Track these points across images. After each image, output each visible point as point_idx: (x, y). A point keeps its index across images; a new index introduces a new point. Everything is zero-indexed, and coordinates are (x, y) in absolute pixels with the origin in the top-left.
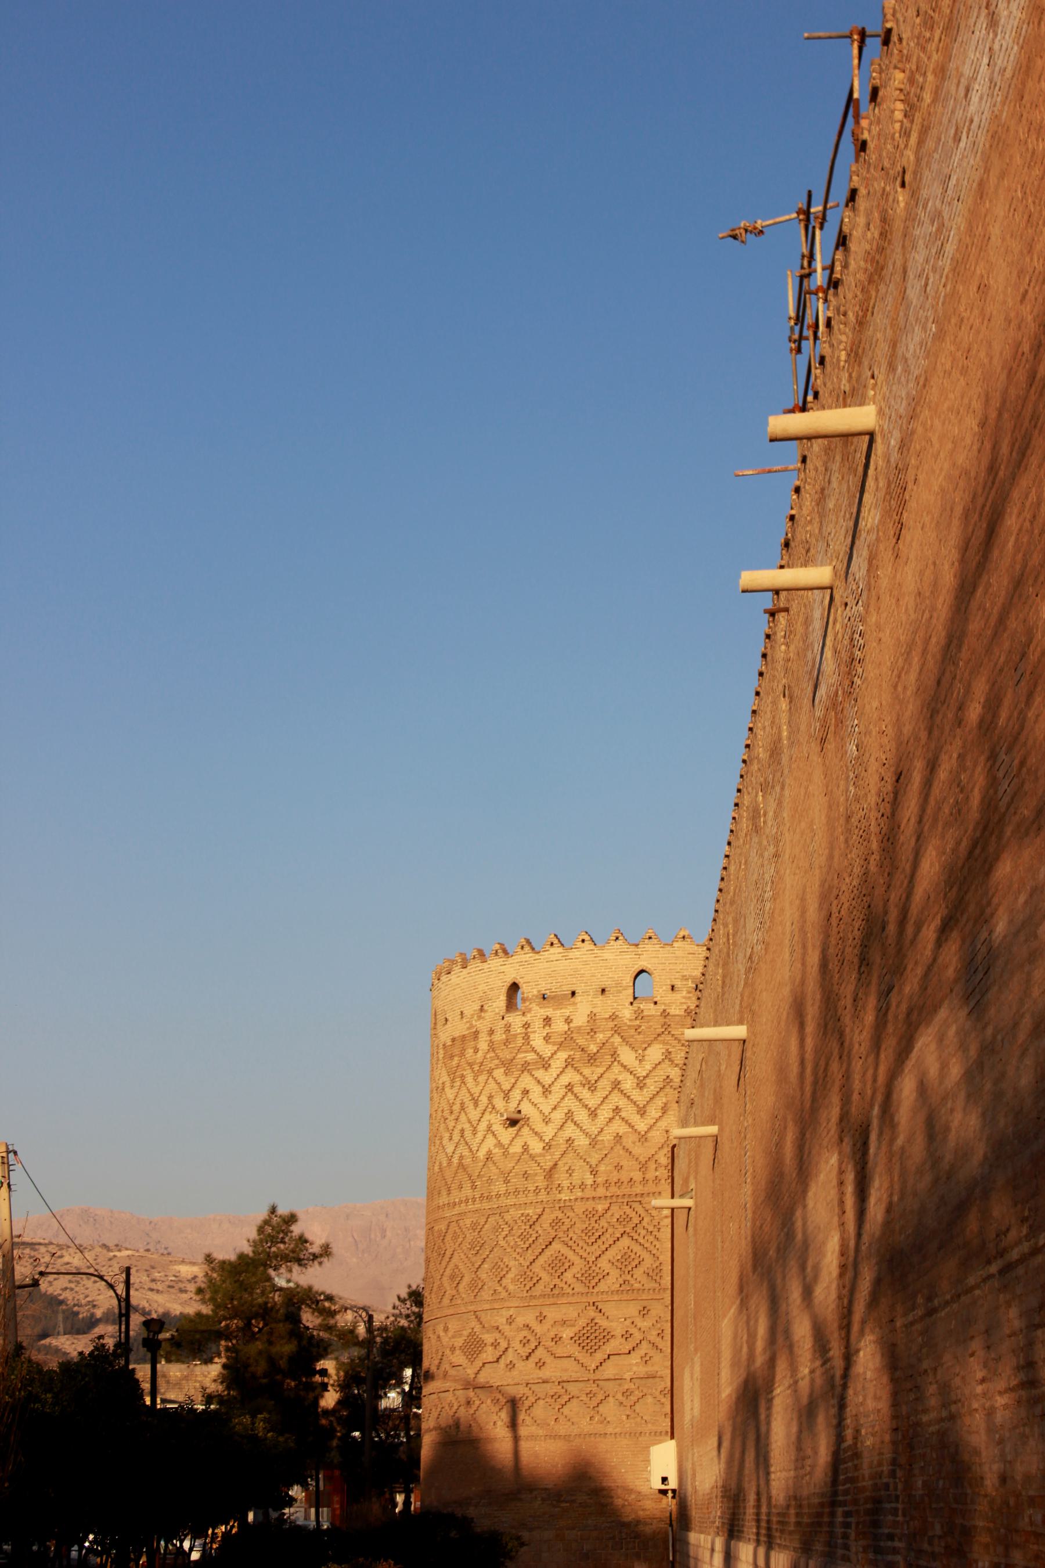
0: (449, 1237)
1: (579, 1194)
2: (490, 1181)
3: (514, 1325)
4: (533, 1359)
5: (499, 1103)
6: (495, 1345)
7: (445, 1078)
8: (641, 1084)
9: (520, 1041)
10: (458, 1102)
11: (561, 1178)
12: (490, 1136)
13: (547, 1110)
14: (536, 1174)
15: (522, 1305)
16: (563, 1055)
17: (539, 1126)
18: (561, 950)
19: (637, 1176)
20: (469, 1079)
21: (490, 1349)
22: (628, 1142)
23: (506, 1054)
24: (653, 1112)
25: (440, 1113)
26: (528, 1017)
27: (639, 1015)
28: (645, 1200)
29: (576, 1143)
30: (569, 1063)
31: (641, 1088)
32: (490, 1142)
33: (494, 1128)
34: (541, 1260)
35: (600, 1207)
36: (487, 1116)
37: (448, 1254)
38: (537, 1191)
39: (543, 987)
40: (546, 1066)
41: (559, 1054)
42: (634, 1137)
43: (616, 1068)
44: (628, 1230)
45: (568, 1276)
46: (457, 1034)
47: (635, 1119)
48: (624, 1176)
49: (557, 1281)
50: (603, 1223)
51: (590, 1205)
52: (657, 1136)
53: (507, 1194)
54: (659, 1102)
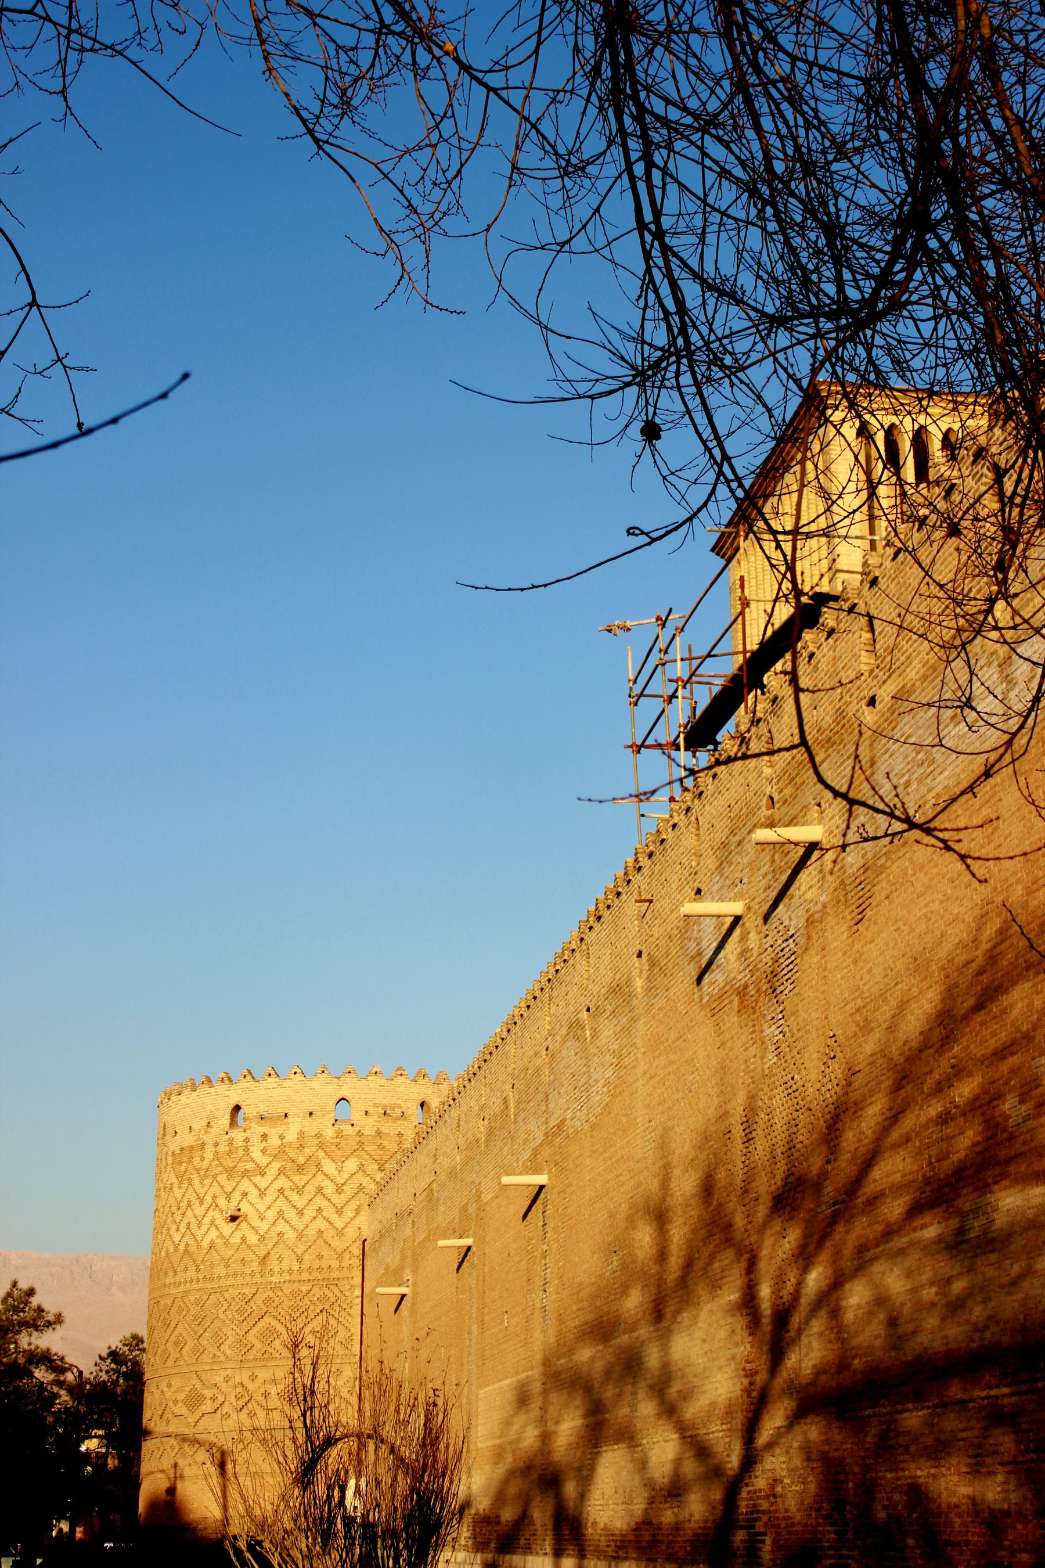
0: (174, 1310)
1: (288, 1278)
2: (212, 1265)
3: (230, 1383)
4: (245, 1411)
5: (222, 1202)
6: (214, 1399)
7: (173, 1179)
8: (339, 1190)
9: (241, 1152)
10: (185, 1200)
11: (273, 1263)
12: (213, 1228)
13: (262, 1208)
16: (276, 1165)
17: (256, 1222)
18: (277, 1079)
19: (335, 1264)
20: (196, 1182)
21: (209, 1402)
22: (328, 1236)
23: (229, 1163)
24: (349, 1213)
25: (167, 1209)
26: (248, 1134)
27: (339, 1134)
28: (340, 1283)
29: (286, 1236)
30: (281, 1172)
31: (340, 1193)
32: (213, 1234)
33: (217, 1222)
34: (254, 1331)
35: (304, 1289)
36: (211, 1213)
37: (173, 1324)
38: (252, 1274)
39: (262, 1109)
40: (262, 1174)
42: (333, 1232)
43: (320, 1177)
44: (326, 1307)
45: (277, 1343)
46: (185, 1145)
47: (334, 1218)
48: (324, 1264)
49: (267, 1348)
50: (306, 1301)
51: (296, 1286)
52: (351, 1232)
53: (227, 1276)
54: (354, 1204)
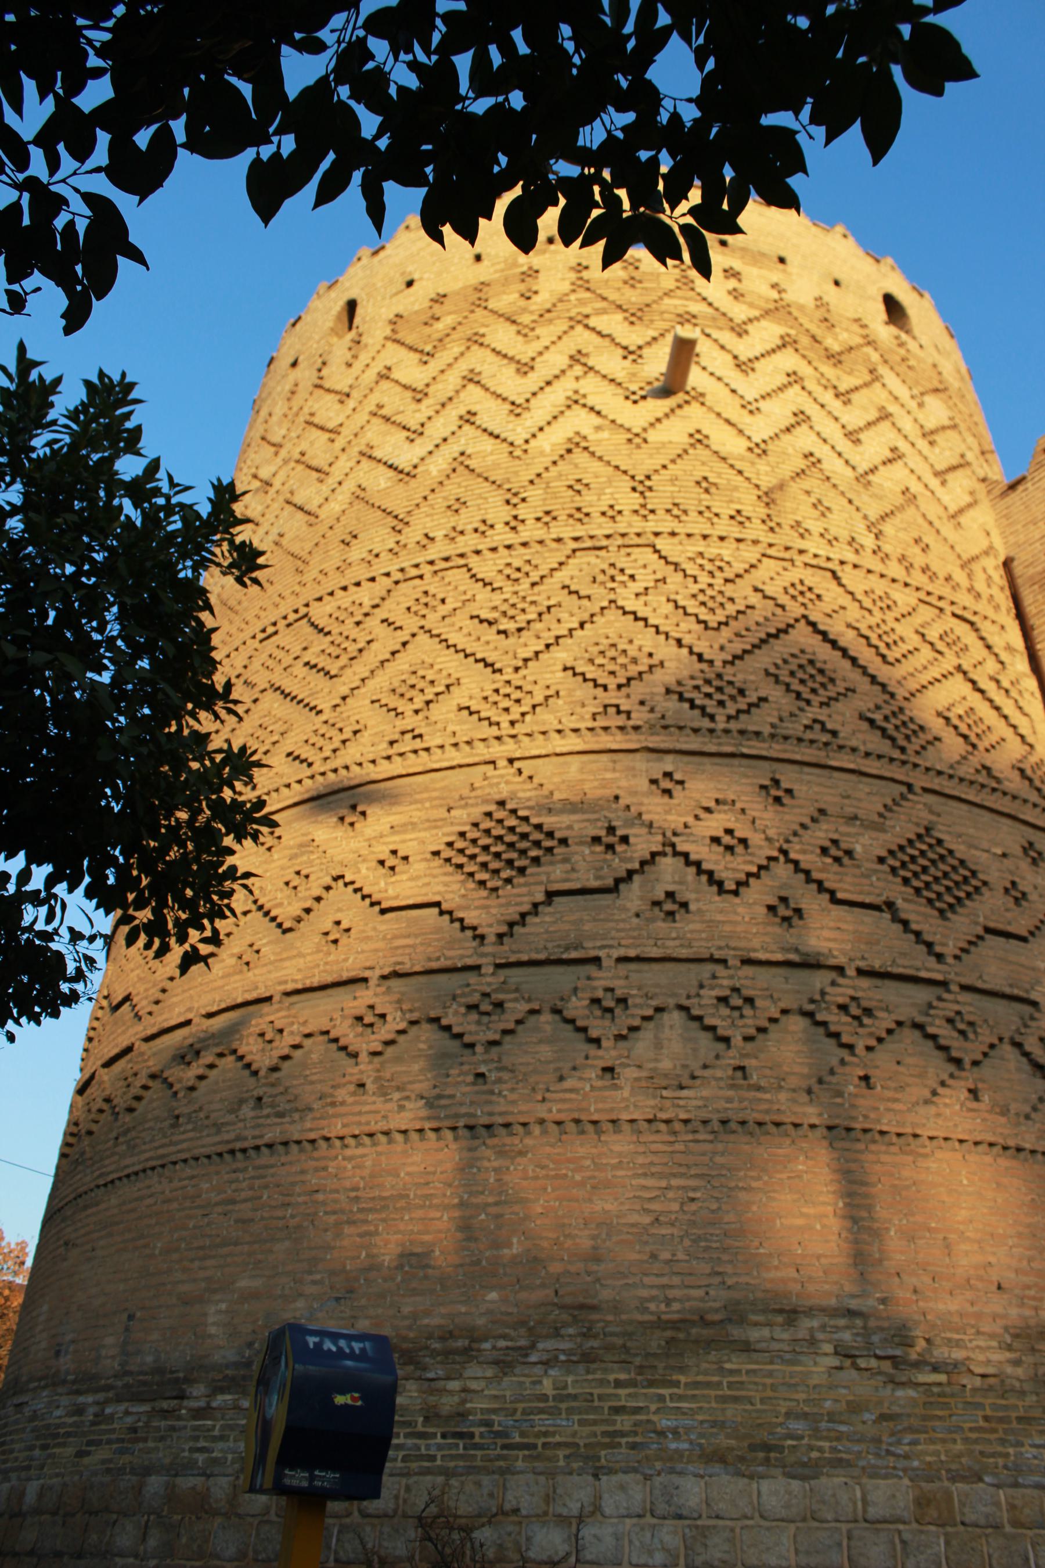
14: (736, 489)
15: (712, 748)
41: (764, 323)
